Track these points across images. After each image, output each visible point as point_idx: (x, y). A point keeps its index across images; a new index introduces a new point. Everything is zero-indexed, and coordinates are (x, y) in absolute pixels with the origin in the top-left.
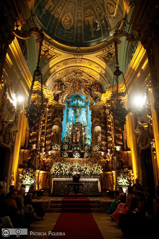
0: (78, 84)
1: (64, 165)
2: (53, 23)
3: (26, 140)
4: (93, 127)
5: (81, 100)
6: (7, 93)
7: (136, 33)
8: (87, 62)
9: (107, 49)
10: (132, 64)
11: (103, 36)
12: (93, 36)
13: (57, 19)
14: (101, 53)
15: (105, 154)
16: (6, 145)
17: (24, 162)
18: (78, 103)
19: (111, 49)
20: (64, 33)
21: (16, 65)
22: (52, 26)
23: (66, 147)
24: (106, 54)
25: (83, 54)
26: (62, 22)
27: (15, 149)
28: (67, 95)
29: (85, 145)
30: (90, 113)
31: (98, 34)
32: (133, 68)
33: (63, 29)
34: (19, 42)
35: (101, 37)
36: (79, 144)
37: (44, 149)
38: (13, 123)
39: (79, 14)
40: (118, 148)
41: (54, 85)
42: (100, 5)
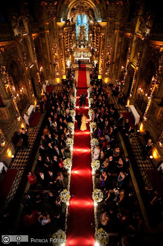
4: (89, 34)
23: (78, 43)
29: (86, 40)
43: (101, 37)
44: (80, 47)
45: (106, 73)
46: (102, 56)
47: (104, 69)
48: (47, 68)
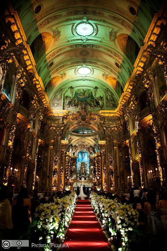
0: (83, 146)
1: (78, 184)
4: (90, 166)
14: (93, 137)
23: (78, 175)
29: (87, 174)
30: (89, 159)
43: (102, 152)
44: (81, 180)
45: (112, 188)
46: (105, 171)
47: (108, 183)
48: (44, 182)
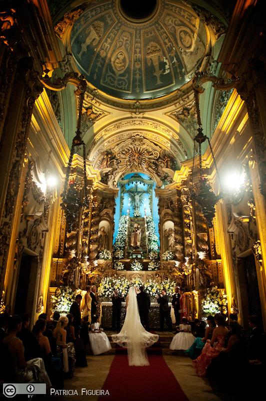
1: (118, 282)
2: (99, 64)
3: (60, 244)
4: (161, 223)
5: (142, 181)
6: (32, 173)
7: (228, 76)
8: (150, 122)
9: (182, 102)
10: (222, 123)
11: (174, 82)
12: (159, 82)
13: (104, 59)
14: (173, 107)
15: (181, 265)
16: (31, 251)
17: (58, 277)
18: (136, 186)
19: (188, 101)
20: (114, 79)
21: (45, 129)
22: (97, 70)
23: (120, 254)
24: (180, 110)
25: (145, 110)
26: (112, 63)
27: (45, 257)
28: (120, 174)
29: (150, 251)
30: (156, 201)
31: (167, 80)
32: (223, 129)
33: (113, 72)
34: (49, 96)
35: (172, 83)
36: (141, 249)
37: (87, 257)
38: (41, 217)
39: (138, 50)
40: (202, 256)
41: (100, 159)
42: (168, 35)
